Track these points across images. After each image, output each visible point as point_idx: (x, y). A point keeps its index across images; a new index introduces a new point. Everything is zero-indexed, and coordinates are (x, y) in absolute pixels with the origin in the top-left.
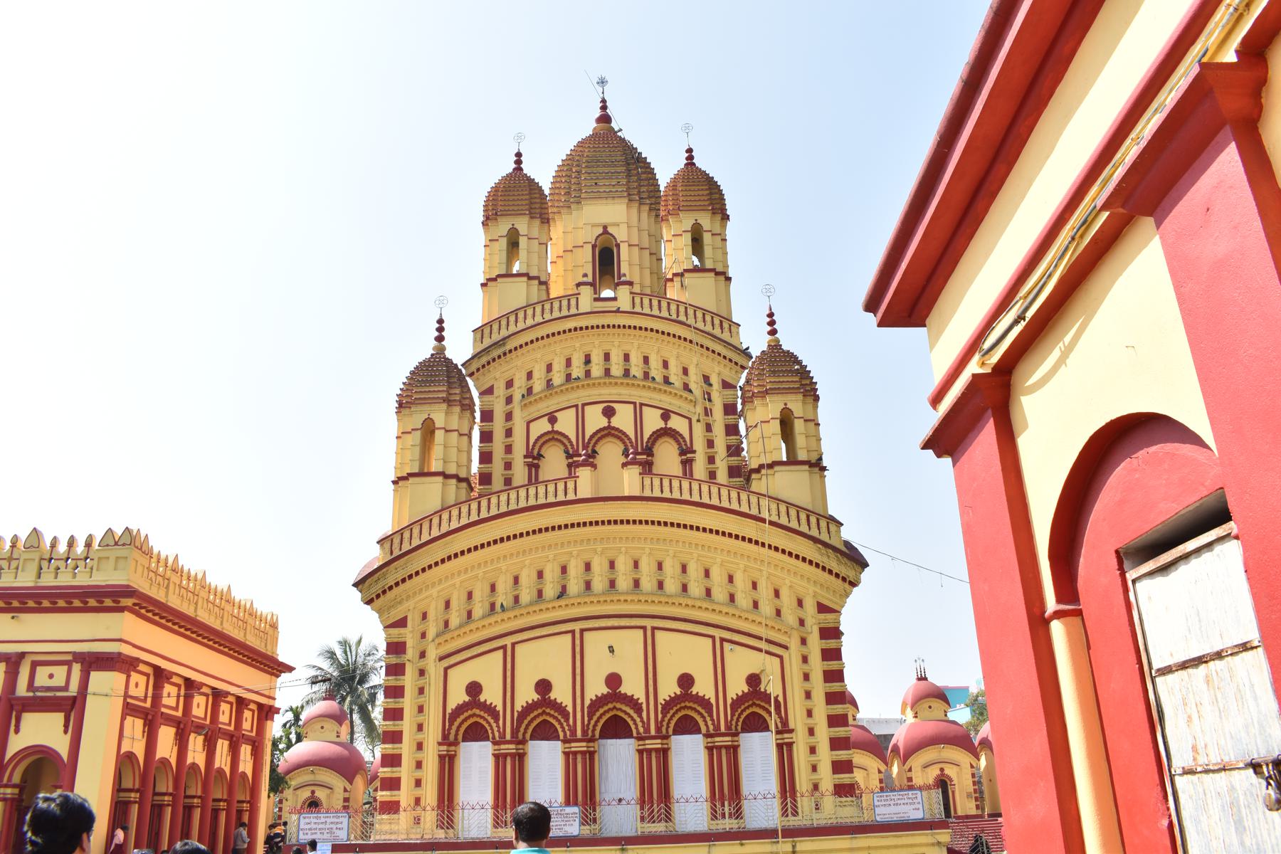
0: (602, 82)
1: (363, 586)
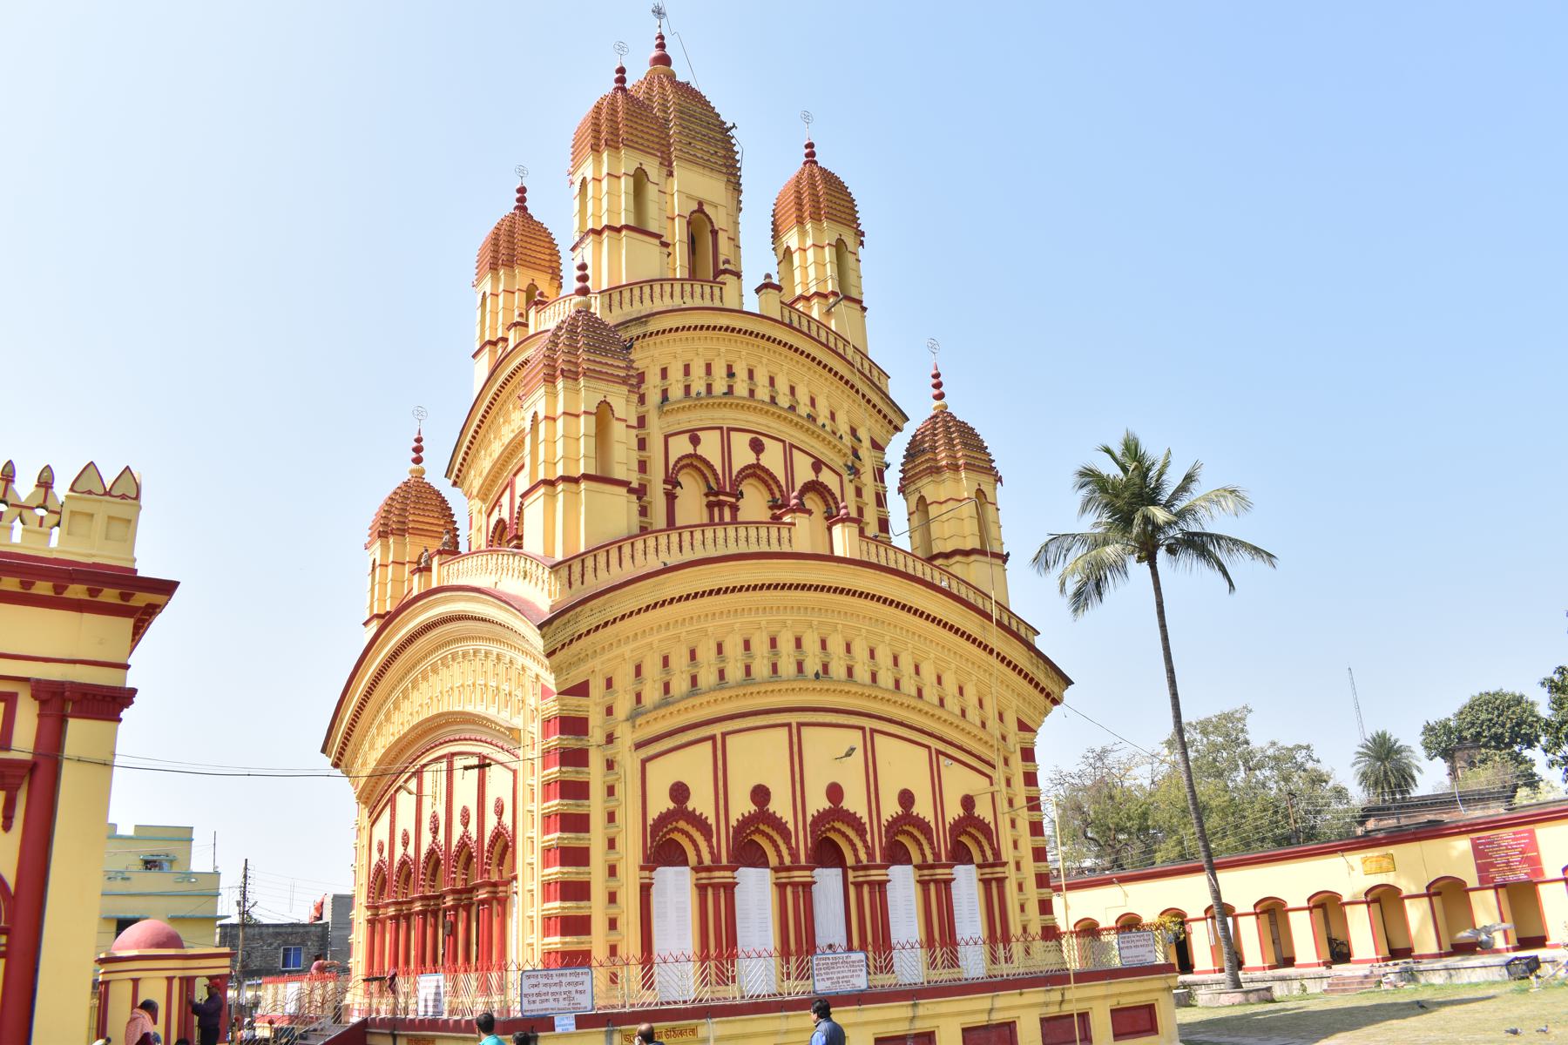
0: (659, 12)
1: (549, 628)
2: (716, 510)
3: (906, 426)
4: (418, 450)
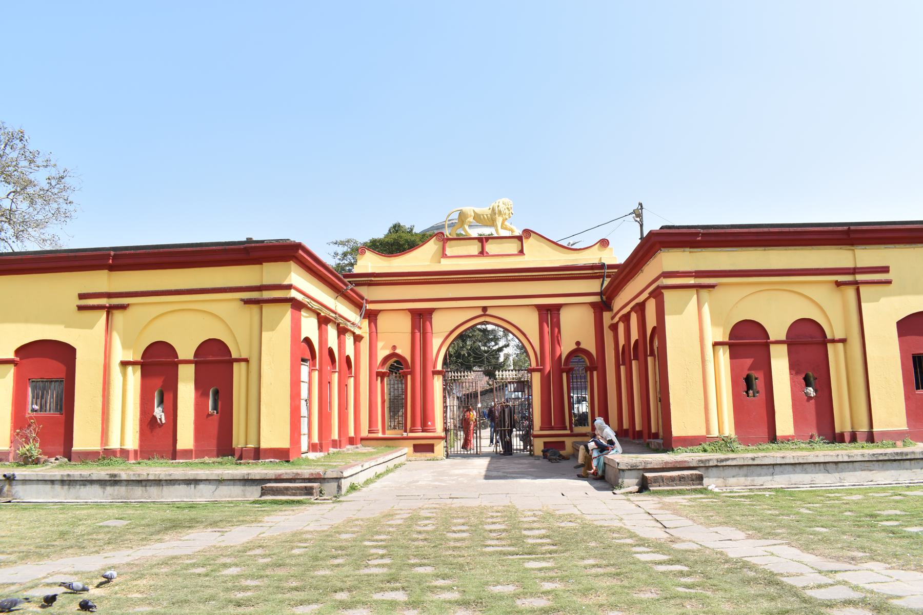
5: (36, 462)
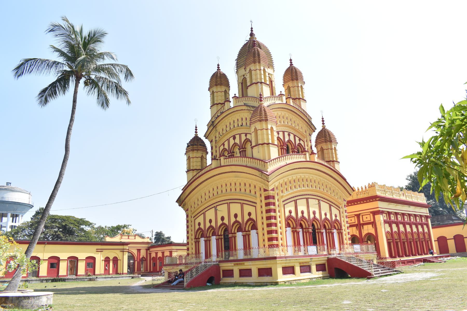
2: (283, 150)
3: (316, 131)
4: (196, 130)
5: (90, 276)
